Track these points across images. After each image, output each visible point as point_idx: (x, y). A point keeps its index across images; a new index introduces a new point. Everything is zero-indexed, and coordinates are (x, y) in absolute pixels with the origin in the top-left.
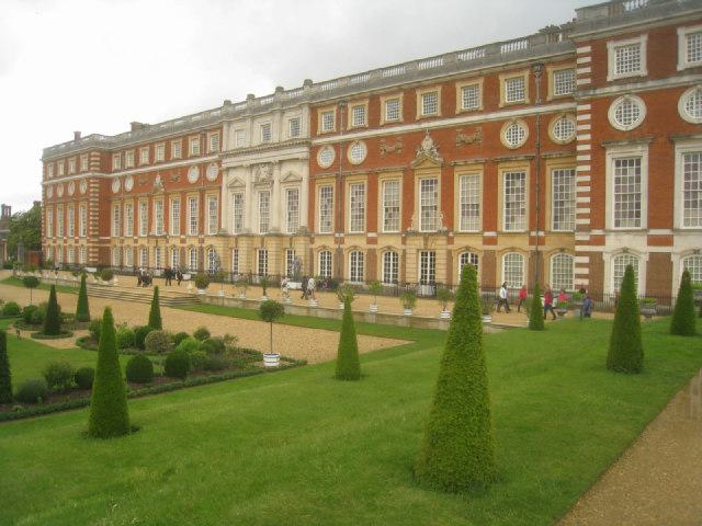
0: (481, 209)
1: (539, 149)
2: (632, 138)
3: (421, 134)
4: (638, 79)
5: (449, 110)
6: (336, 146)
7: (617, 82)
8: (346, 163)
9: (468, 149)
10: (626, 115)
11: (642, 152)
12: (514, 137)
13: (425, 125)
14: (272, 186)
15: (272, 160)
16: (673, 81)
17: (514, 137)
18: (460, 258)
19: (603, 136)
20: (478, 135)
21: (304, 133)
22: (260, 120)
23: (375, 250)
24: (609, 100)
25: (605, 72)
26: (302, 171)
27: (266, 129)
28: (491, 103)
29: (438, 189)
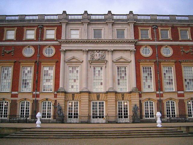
6: (152, 46)
14: (106, 64)
15: (108, 49)
18: (42, 104)
21: (134, 38)
22: (94, 26)
23: (183, 100)
26: (132, 57)
27: (97, 33)
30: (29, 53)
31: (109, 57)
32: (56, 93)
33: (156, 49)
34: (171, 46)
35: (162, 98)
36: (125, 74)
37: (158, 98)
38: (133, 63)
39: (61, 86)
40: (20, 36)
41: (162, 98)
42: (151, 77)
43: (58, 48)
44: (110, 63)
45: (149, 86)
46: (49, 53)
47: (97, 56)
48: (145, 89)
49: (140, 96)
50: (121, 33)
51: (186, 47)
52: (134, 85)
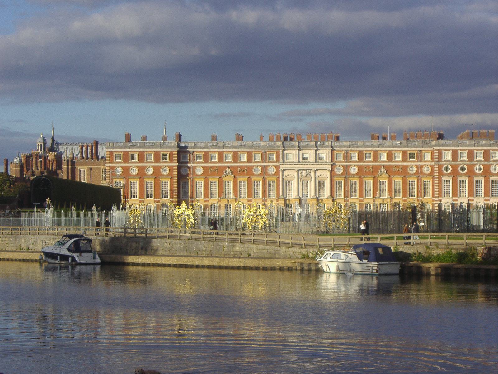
0: (401, 191)
3: (380, 166)
4: (449, 161)
6: (343, 166)
7: (445, 161)
8: (349, 173)
9: (396, 173)
11: (451, 179)
13: (382, 164)
16: (458, 163)
19: (441, 174)
20: (400, 168)
24: (443, 165)
25: (442, 158)
26: (328, 174)
30: (258, 171)
32: (278, 199)
33: (346, 168)
34: (357, 166)
35: (348, 203)
36: (324, 186)
37: (346, 203)
38: (329, 179)
39: (281, 194)
40: (250, 158)
41: (348, 203)
42: (342, 188)
43: (277, 168)
44: (313, 179)
45: (340, 194)
49: (333, 200)
52: (329, 194)
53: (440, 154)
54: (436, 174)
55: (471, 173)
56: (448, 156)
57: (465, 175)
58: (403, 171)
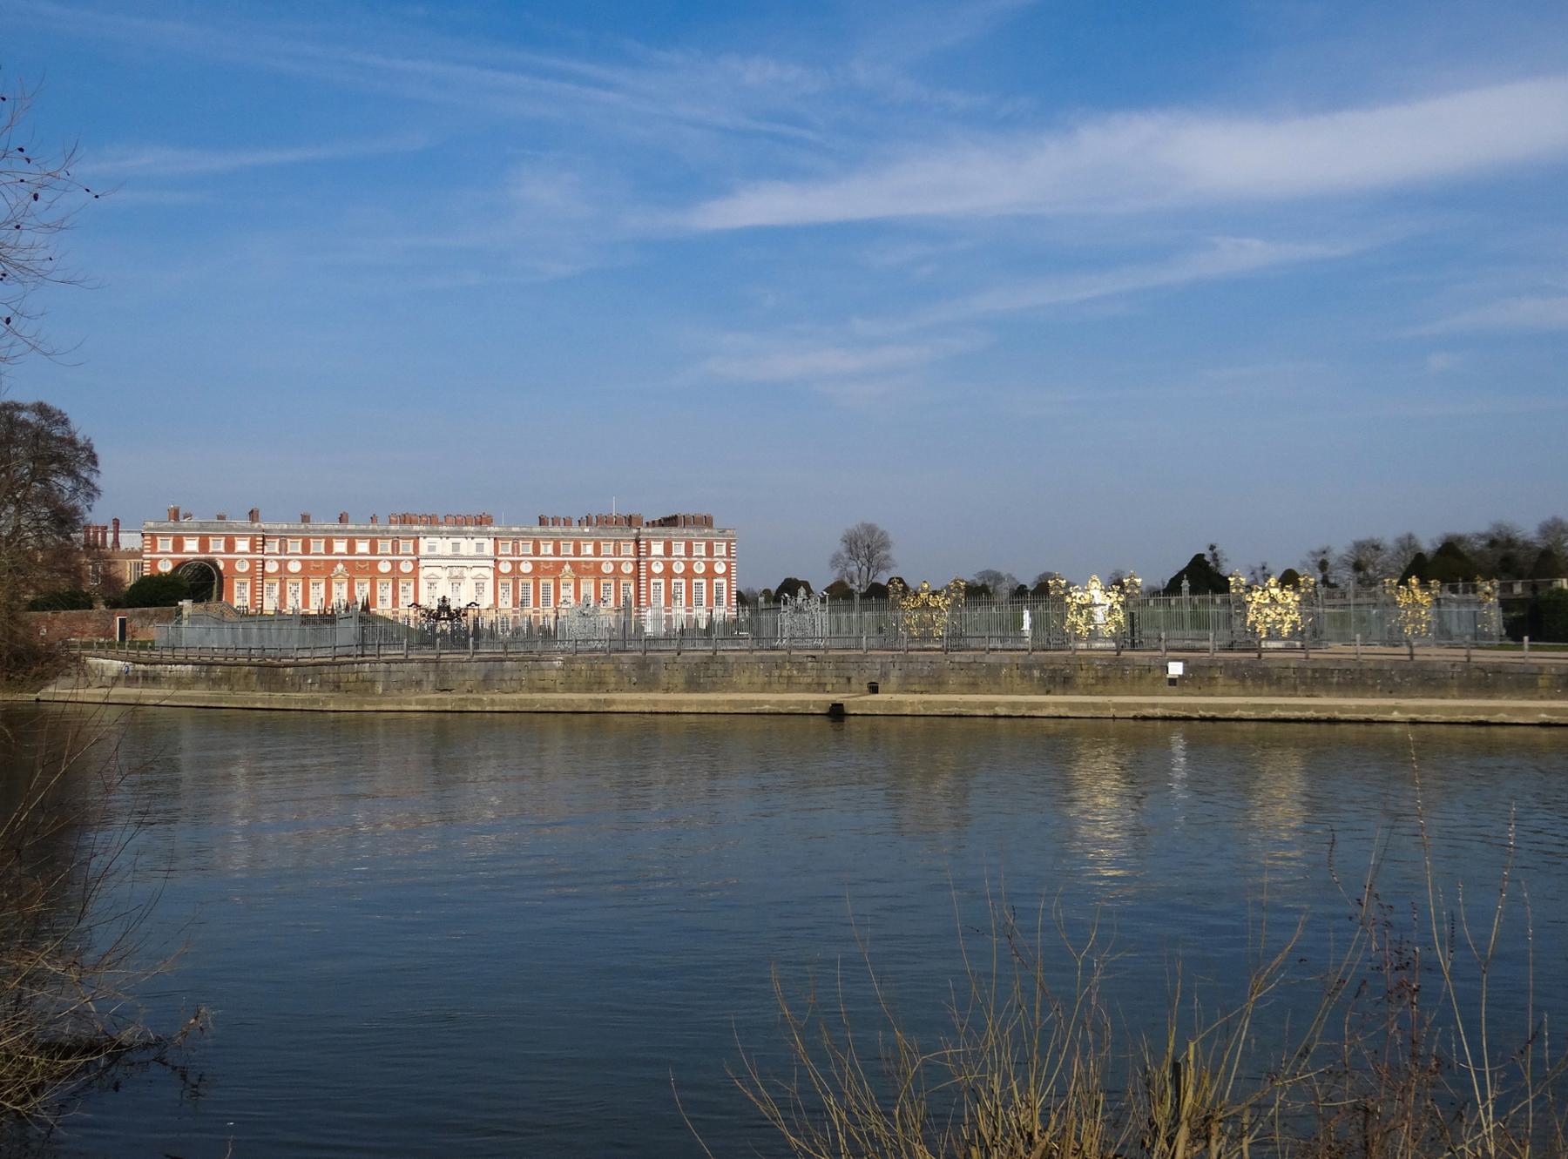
1: (617, 573)
2: (660, 575)
5: (577, 552)
8: (519, 572)
9: (587, 573)
10: (658, 568)
12: (608, 568)
17: (608, 568)
19: (650, 575)
26: (490, 574)
27: (456, 546)
28: (597, 552)
29: (572, 587)
30: (385, 567)
31: (466, 573)
33: (516, 565)
43: (416, 563)
46: (406, 568)
47: (456, 572)
48: (501, 605)
50: (480, 546)
51: (547, 563)
53: (649, 547)
54: (643, 574)
55: (689, 574)
56: (657, 549)
57: (682, 575)
58: (596, 572)
